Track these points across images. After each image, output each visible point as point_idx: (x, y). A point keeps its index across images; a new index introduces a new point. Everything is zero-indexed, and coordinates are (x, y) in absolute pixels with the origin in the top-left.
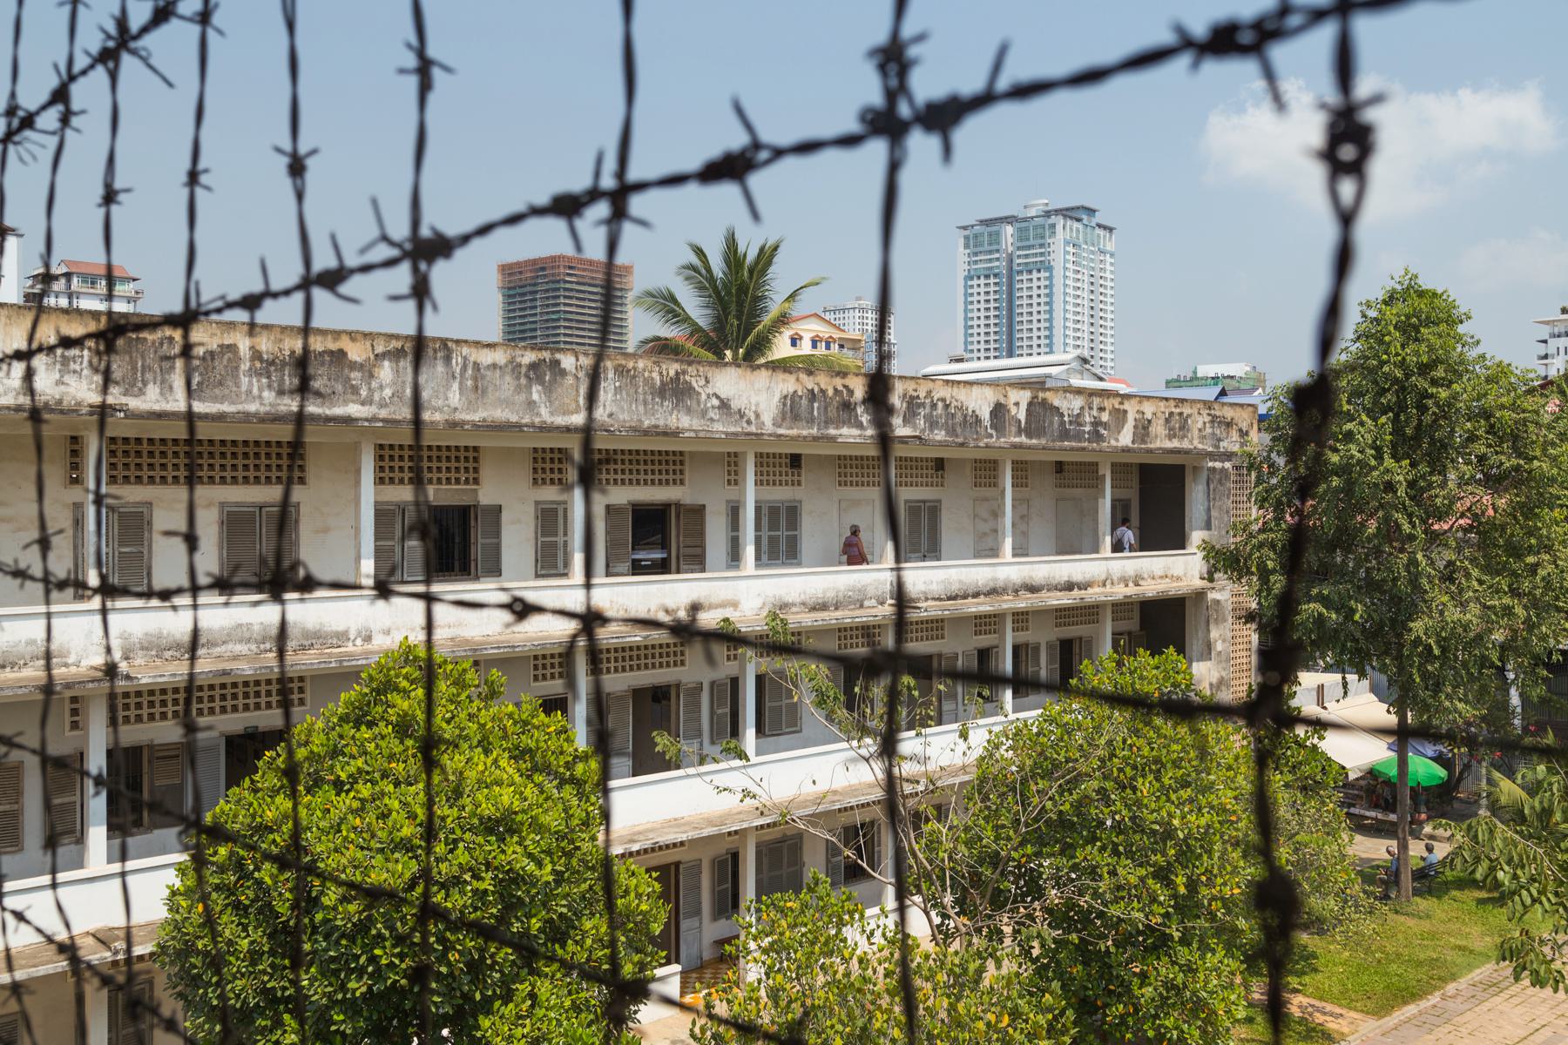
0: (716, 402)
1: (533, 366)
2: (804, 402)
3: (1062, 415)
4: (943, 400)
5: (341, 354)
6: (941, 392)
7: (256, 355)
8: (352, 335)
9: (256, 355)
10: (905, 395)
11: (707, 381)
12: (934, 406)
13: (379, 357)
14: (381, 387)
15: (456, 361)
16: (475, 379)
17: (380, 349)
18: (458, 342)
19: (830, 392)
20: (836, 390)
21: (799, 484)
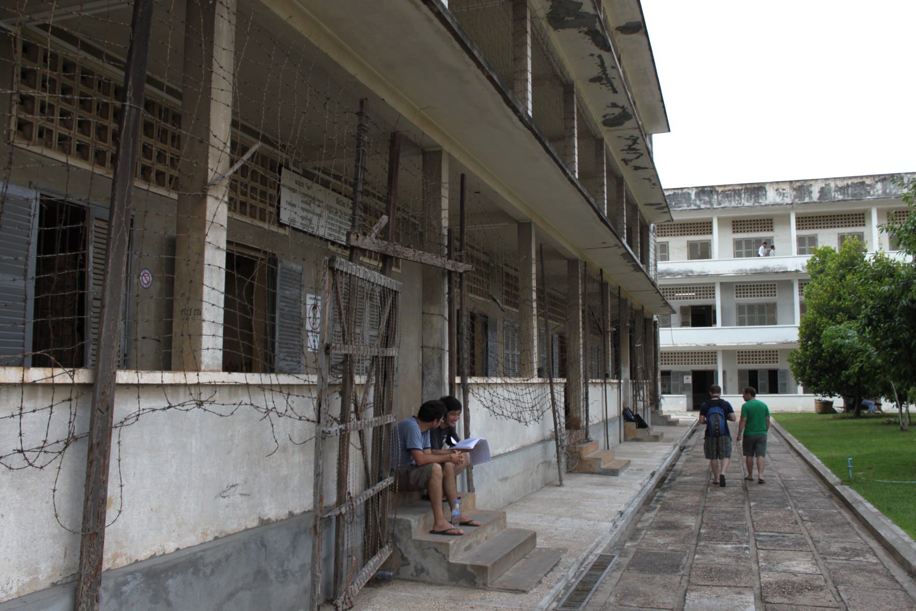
5: (863, 183)
7: (836, 186)
8: (867, 177)
9: (836, 186)
13: (877, 182)
14: (877, 191)
17: (877, 179)
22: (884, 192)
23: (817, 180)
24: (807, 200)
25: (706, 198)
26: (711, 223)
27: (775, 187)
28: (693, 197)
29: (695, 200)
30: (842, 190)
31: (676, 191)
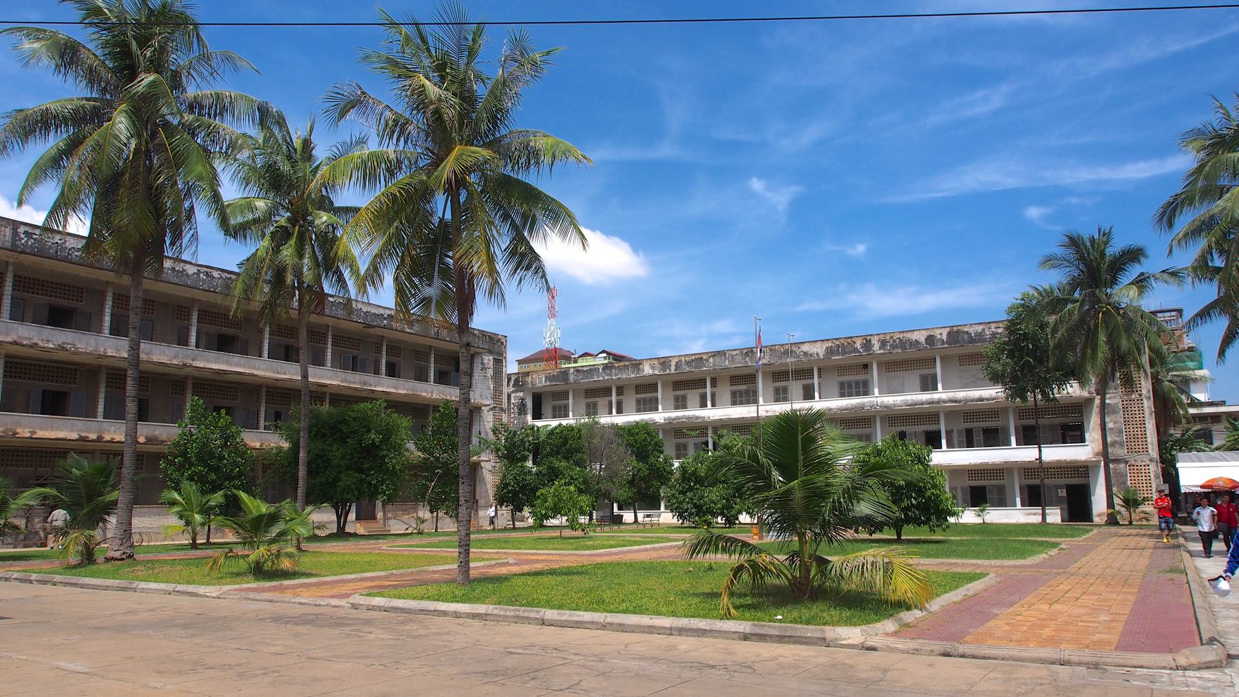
0: (802, 353)
1: (746, 353)
2: (835, 348)
3: (971, 334)
4: (899, 338)
6: (901, 336)
7: (685, 360)
8: (703, 353)
9: (685, 360)
10: (879, 340)
11: (799, 348)
12: (895, 341)
15: (727, 355)
16: (732, 358)
18: (728, 351)
19: (846, 344)
20: (848, 343)
21: (868, 373)
22: (714, 365)
23: (674, 356)
24: (668, 372)
25: (608, 372)
26: (611, 388)
27: (649, 362)
28: (601, 371)
29: (602, 373)
30: (688, 363)
31: (591, 367)
